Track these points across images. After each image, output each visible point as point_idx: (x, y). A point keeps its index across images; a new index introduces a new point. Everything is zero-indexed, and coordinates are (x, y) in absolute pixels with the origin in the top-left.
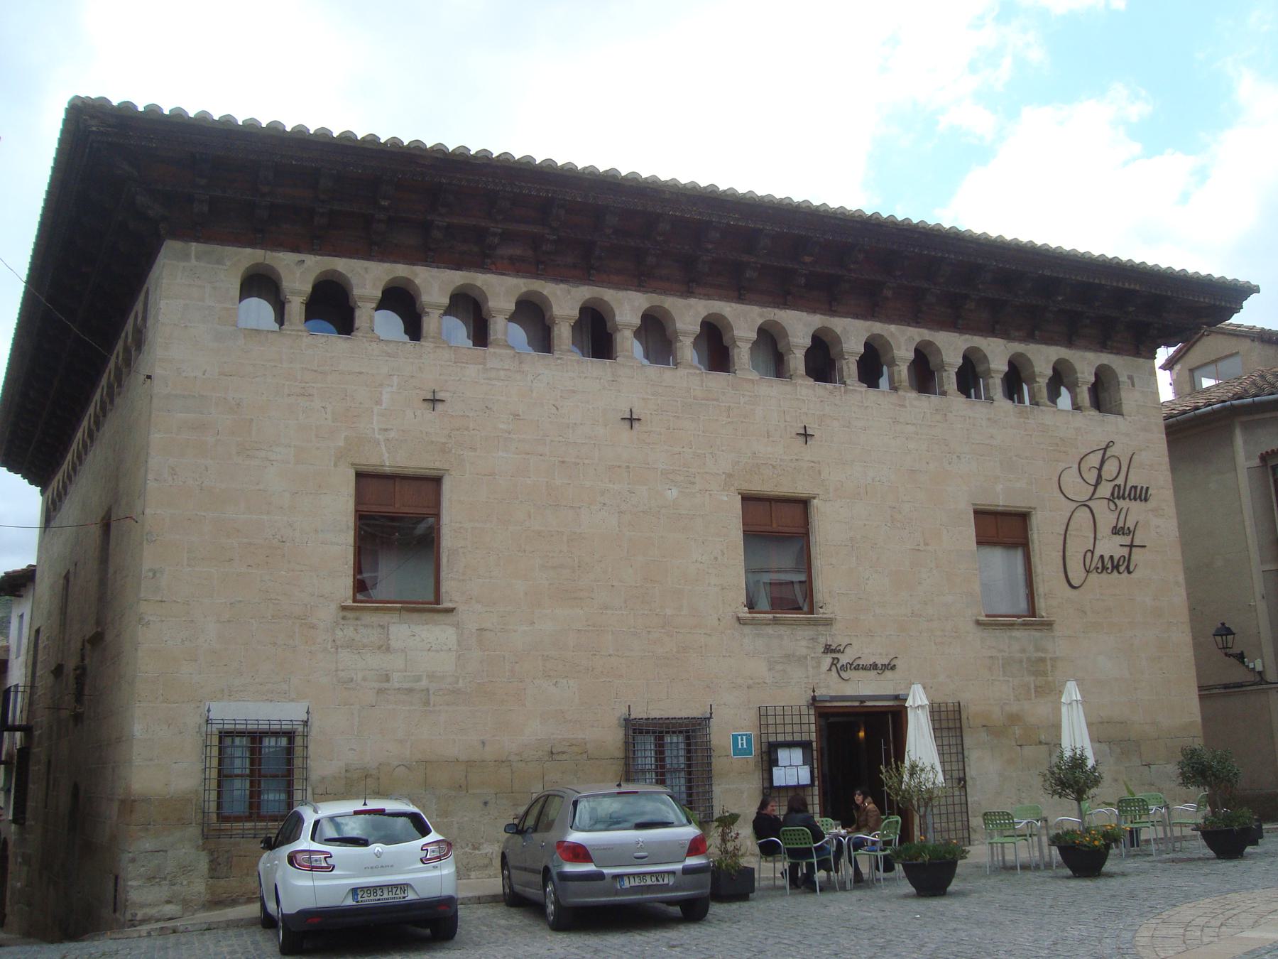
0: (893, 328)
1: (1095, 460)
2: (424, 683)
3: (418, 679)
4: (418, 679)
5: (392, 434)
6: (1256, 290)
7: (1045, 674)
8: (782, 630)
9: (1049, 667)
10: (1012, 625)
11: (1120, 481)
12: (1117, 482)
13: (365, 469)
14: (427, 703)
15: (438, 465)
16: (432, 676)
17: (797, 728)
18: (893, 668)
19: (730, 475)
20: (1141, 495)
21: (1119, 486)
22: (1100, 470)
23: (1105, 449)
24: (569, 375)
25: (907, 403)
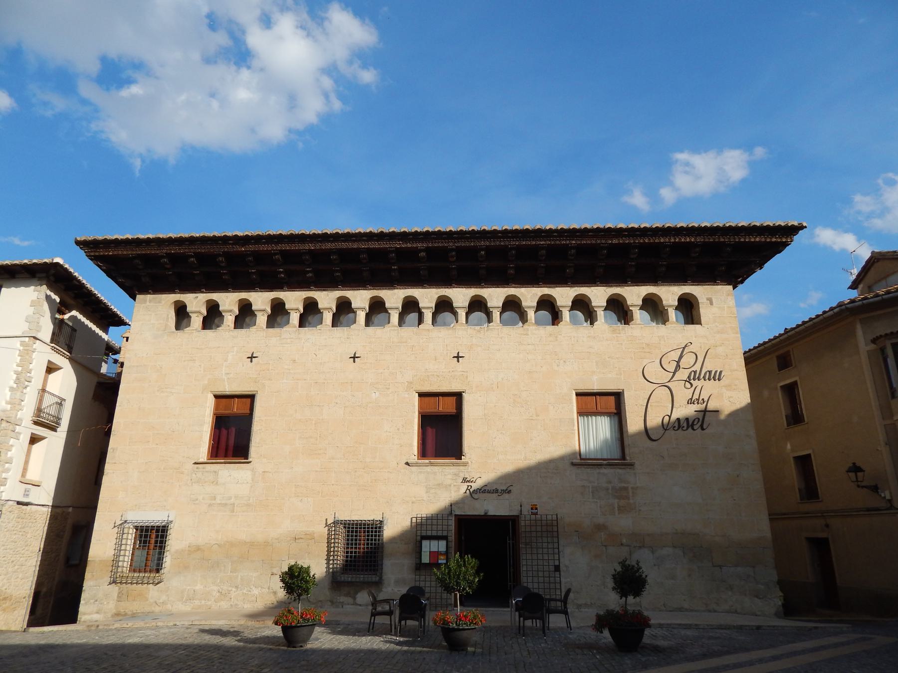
0: (523, 290)
1: (675, 356)
2: (232, 500)
3: (230, 498)
4: (230, 498)
5: (231, 375)
6: (78, 243)
7: (628, 498)
8: (436, 469)
9: (631, 494)
10: (601, 465)
11: (697, 368)
12: (693, 369)
13: (220, 393)
14: (233, 511)
15: (252, 389)
16: (236, 497)
17: (440, 527)
18: (509, 492)
19: (411, 383)
20: (716, 376)
21: (695, 372)
22: (678, 362)
23: (684, 348)
24: (325, 337)
25: (529, 333)
